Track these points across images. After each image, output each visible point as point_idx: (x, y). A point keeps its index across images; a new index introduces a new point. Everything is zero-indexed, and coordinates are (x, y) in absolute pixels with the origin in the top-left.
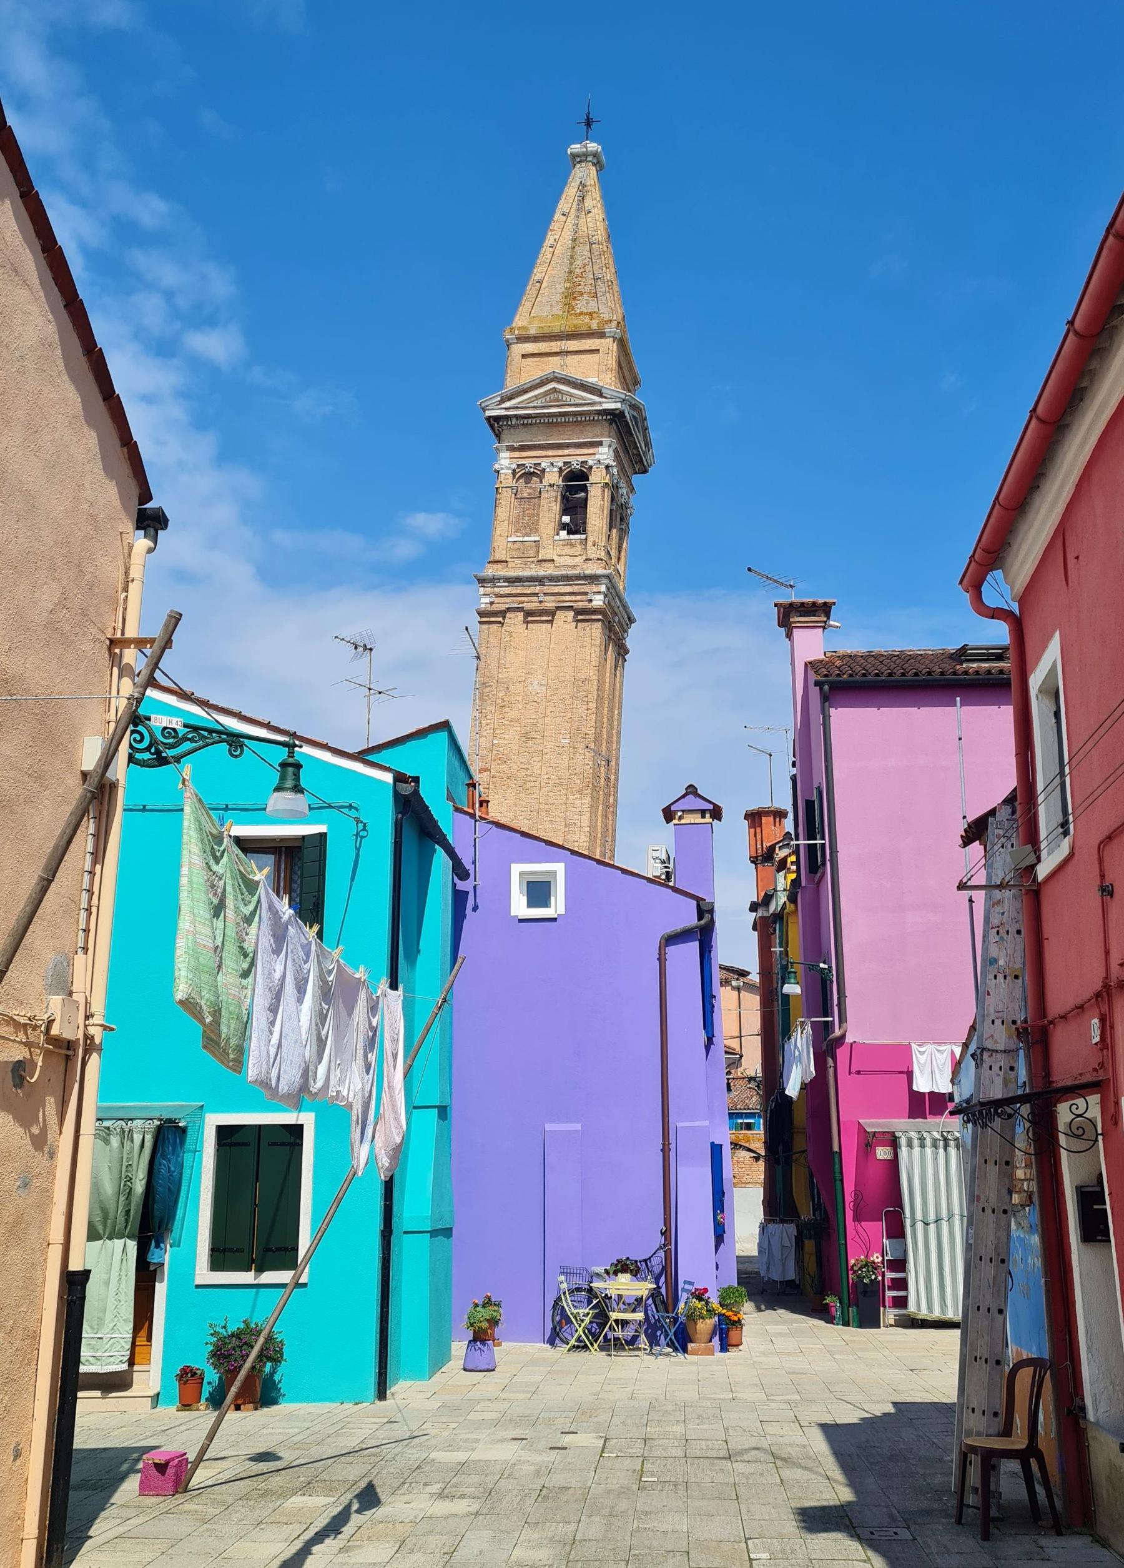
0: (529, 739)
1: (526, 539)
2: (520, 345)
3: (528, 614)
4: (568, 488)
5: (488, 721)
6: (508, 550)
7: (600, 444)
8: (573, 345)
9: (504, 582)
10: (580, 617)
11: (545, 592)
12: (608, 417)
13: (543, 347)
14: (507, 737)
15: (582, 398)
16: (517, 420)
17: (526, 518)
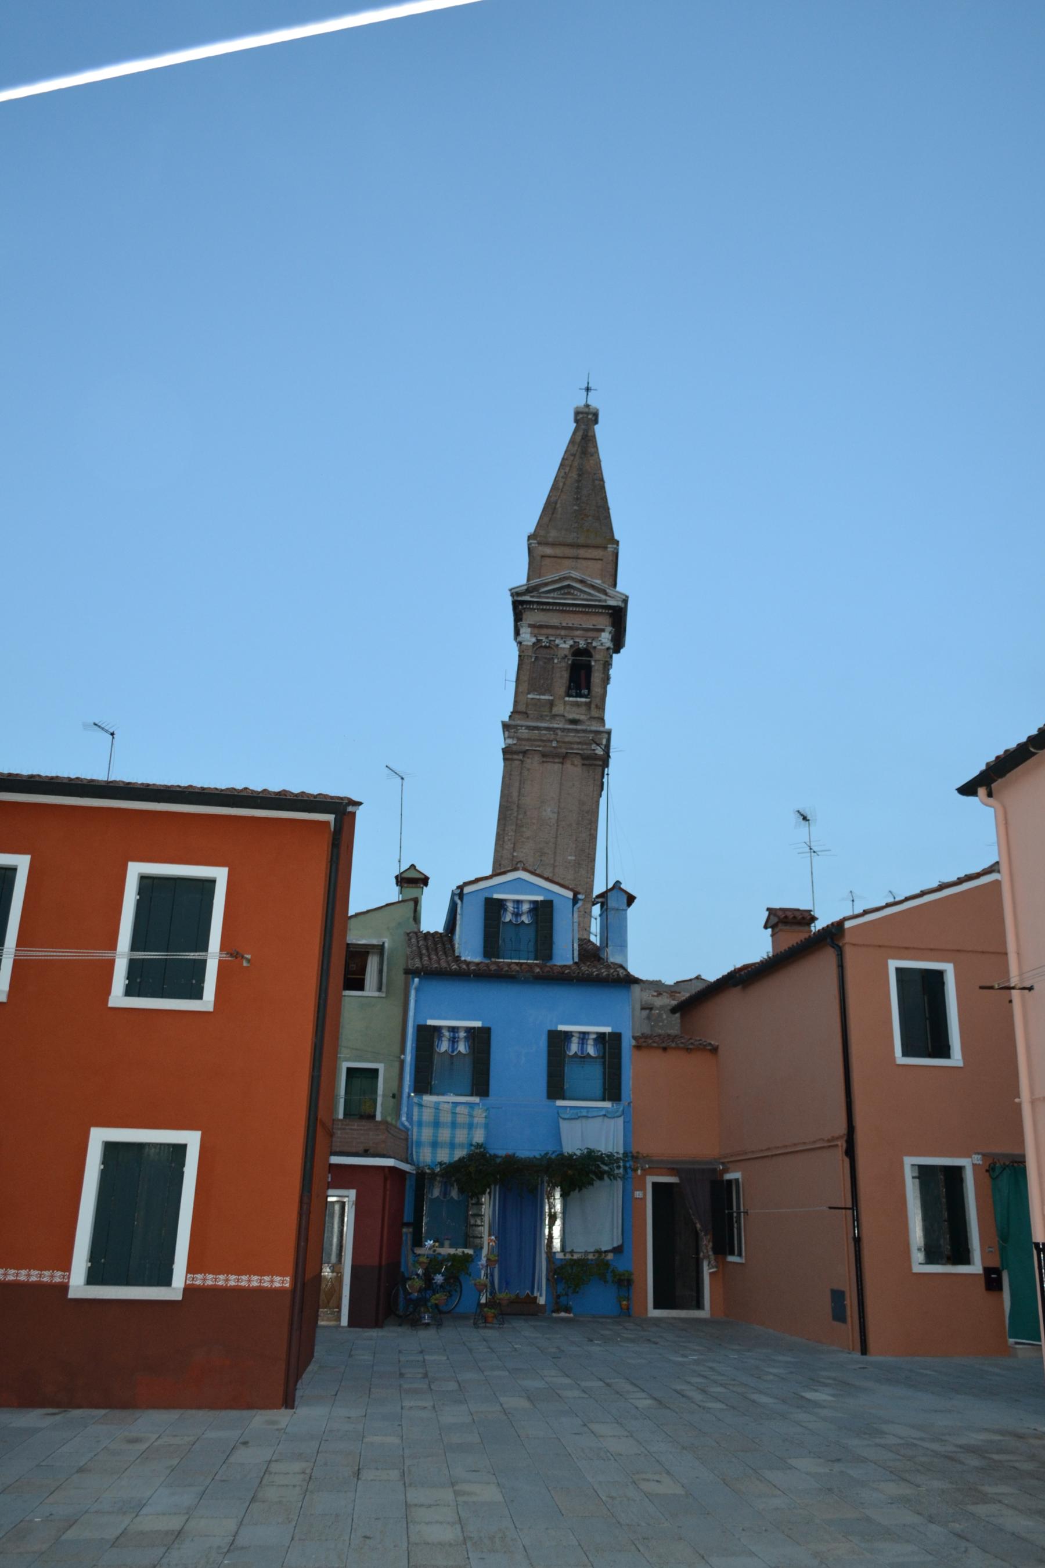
0: (543, 854)
1: (543, 697)
2: (540, 548)
3: (544, 755)
6: (527, 705)
7: (603, 630)
8: (582, 553)
9: (525, 729)
10: (586, 762)
11: (558, 740)
12: (610, 611)
13: (559, 551)
14: (524, 851)
15: (589, 594)
17: (542, 682)
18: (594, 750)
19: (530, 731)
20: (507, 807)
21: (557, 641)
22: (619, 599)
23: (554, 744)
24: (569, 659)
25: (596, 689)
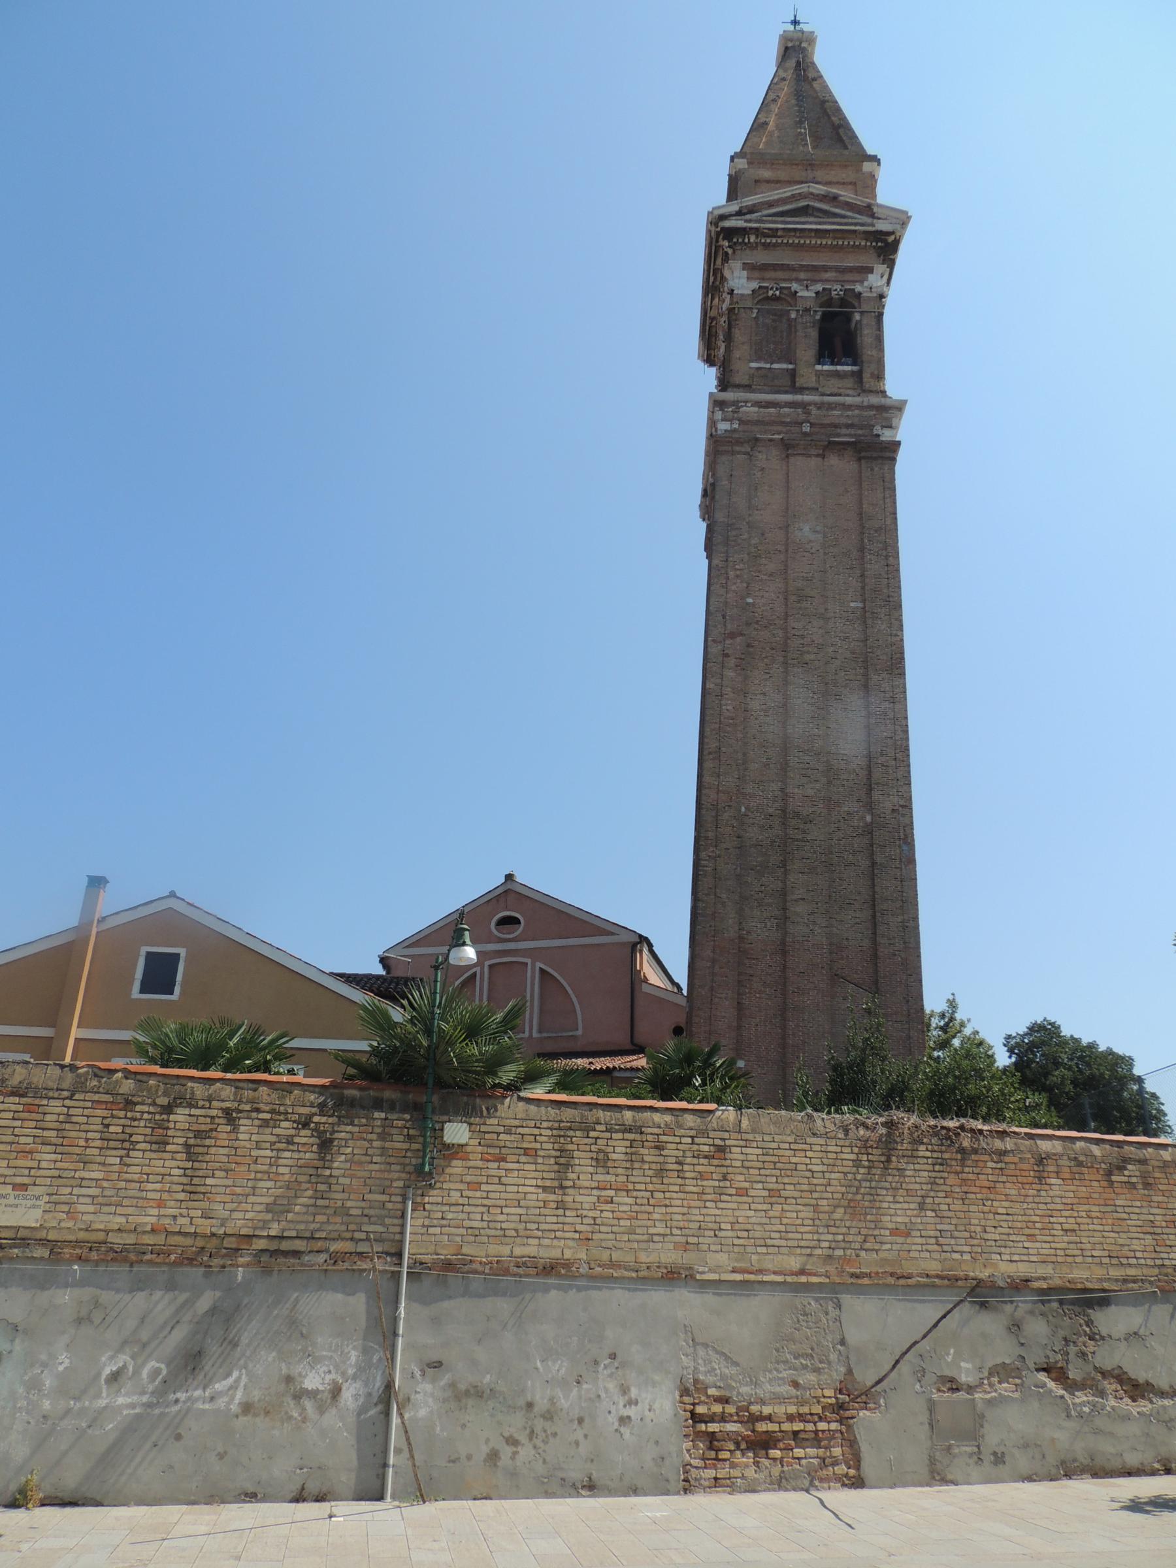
1: (775, 366)
4: (825, 316)
5: (738, 572)
6: (752, 377)
12: (879, 244)
16: (757, 237)
18: (878, 436)
19: (761, 410)
20: (728, 525)
21: (795, 286)
22: (894, 221)
23: (806, 428)
24: (816, 311)
25: (868, 352)
